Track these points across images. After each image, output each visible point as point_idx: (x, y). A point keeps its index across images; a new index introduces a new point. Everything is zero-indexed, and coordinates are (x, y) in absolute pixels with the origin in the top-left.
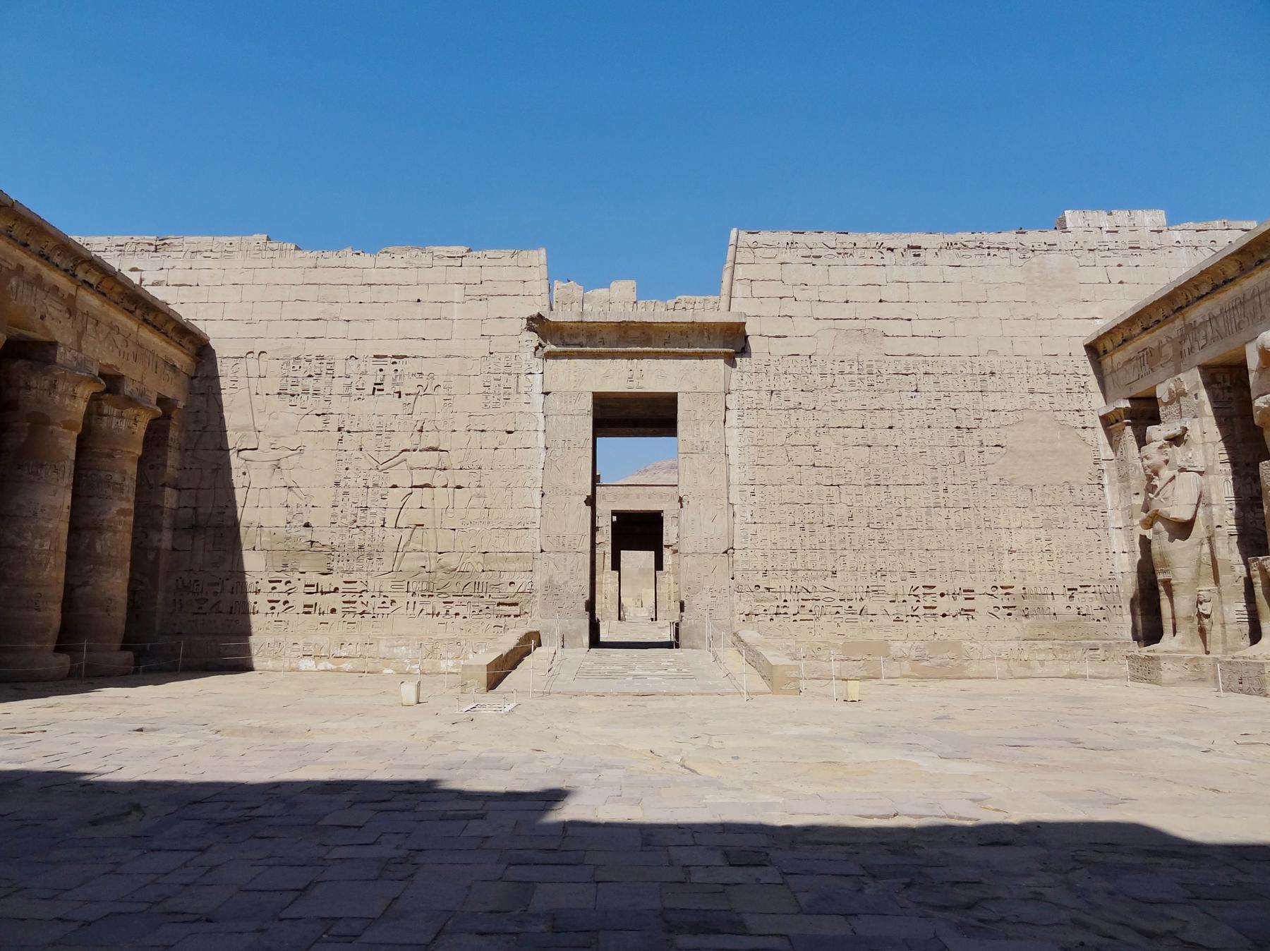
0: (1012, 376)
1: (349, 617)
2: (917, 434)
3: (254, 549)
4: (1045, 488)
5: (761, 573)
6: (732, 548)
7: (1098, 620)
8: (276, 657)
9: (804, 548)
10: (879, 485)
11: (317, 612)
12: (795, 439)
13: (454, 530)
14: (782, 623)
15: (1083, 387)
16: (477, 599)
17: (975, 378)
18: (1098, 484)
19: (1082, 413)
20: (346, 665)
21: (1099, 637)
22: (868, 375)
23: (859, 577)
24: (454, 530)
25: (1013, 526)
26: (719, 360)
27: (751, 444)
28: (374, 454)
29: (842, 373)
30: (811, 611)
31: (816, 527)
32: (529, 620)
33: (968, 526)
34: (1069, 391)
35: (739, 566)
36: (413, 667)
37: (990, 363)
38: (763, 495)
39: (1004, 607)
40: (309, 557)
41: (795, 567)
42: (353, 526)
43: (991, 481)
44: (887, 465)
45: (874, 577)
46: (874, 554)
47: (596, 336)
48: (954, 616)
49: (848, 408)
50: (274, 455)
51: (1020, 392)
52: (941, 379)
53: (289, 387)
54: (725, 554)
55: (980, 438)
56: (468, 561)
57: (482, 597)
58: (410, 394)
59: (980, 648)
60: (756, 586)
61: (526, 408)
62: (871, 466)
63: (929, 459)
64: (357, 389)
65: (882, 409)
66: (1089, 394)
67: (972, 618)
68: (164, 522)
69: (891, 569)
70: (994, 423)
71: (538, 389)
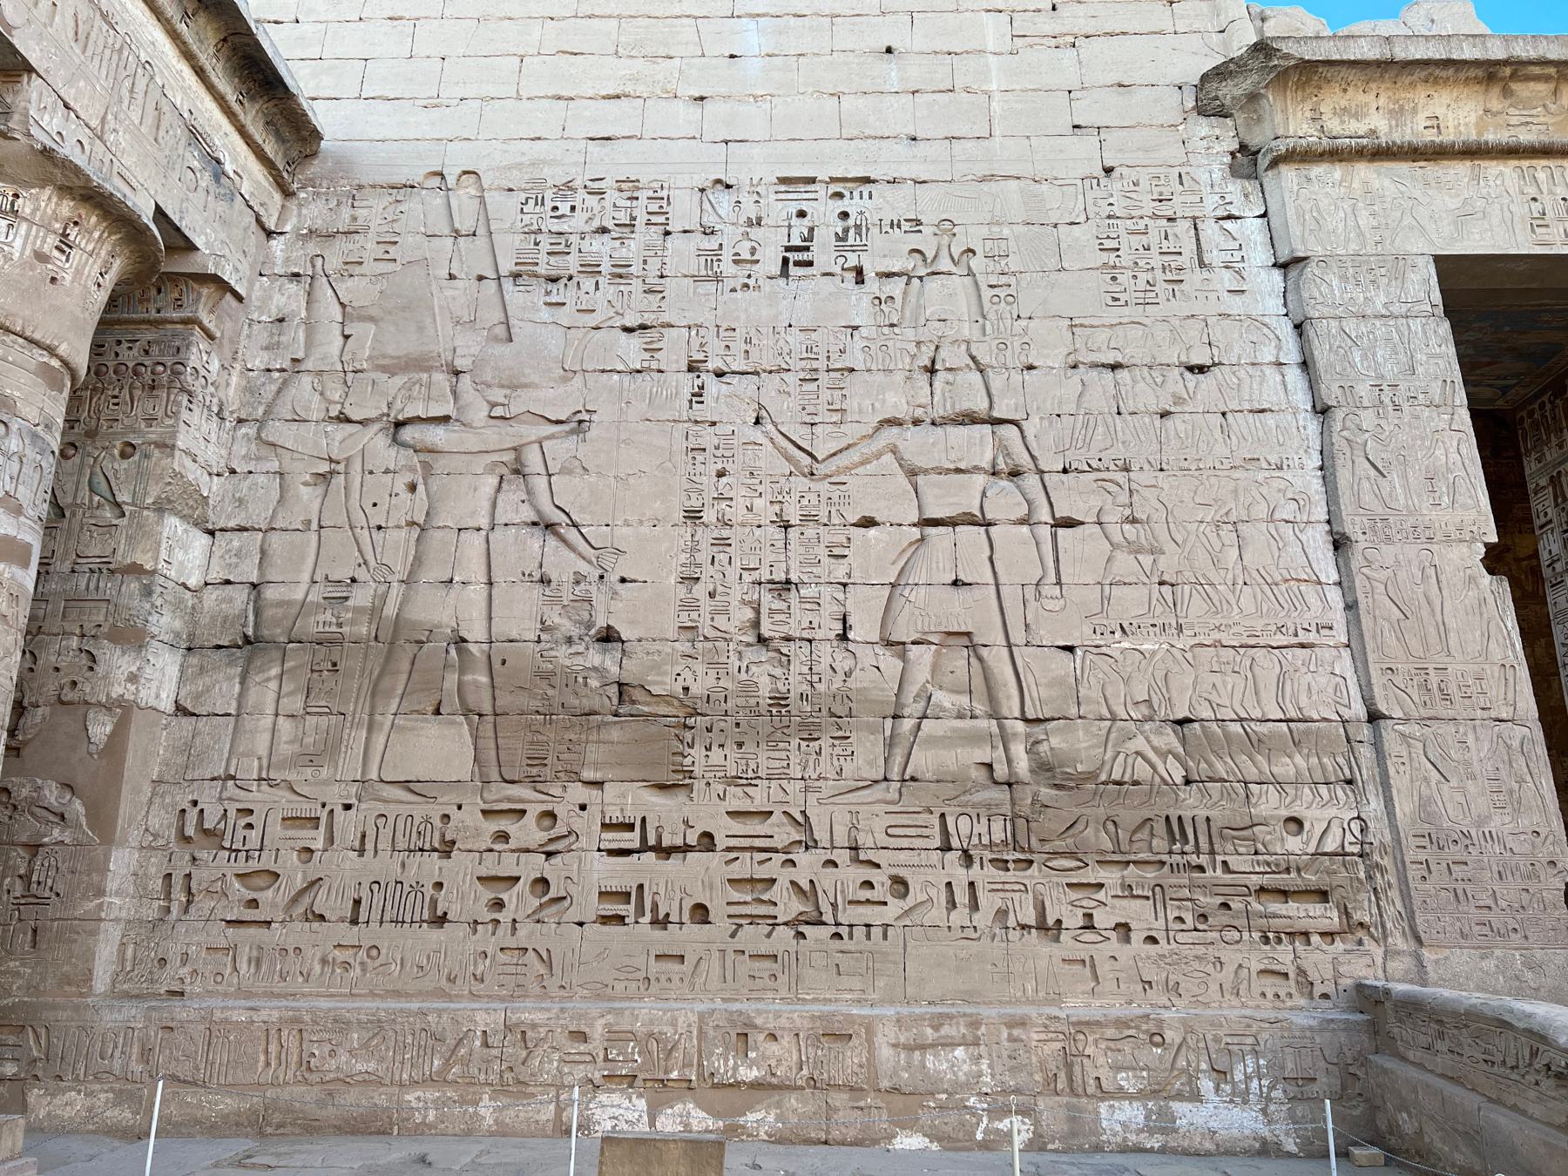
1: (751, 936)
3: (437, 712)
8: (515, 1087)
11: (648, 918)
13: (1070, 649)
16: (1183, 878)
20: (759, 1116)
24: (1070, 649)
28: (800, 434)
32: (1378, 952)
36: (1001, 1126)
40: (615, 734)
42: (744, 638)
47: (1415, 111)
50: (497, 436)
53: (543, 258)
56: (1132, 746)
57: (1201, 869)
58: (889, 275)
61: (1235, 305)
64: (735, 262)
68: (154, 618)
71: (1260, 255)
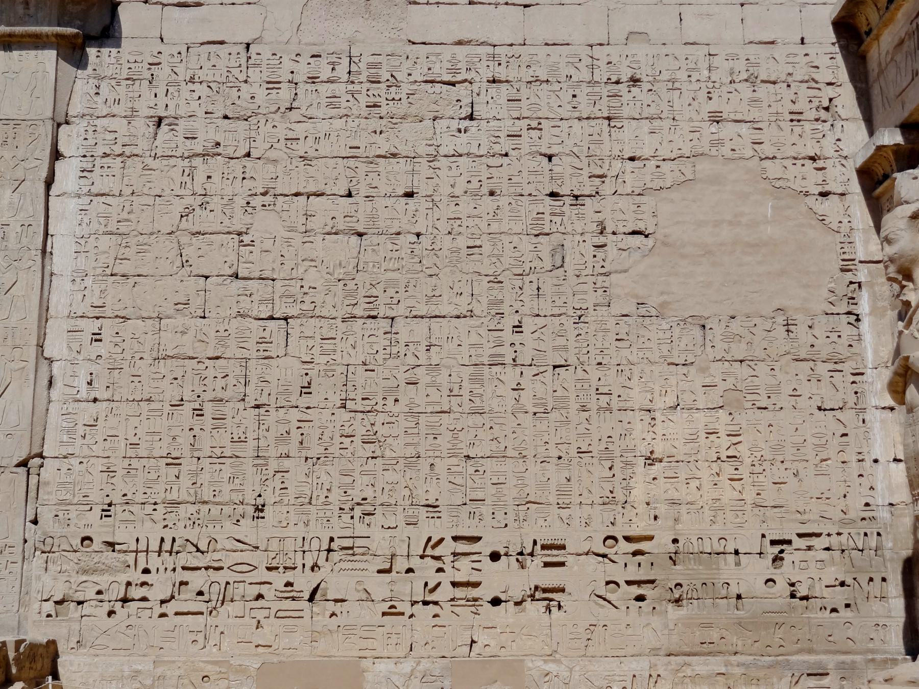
0: (677, 85)
2: (466, 207)
4: (735, 326)
5: (97, 510)
6: (41, 456)
7: (834, 610)
9: (196, 454)
10: (374, 317)
12: (203, 220)
14: (133, 621)
15: (827, 109)
17: (597, 89)
18: (849, 313)
19: (820, 164)
21: (833, 647)
22: (368, 85)
23: (313, 517)
25: (659, 404)
26: (46, 52)
27: (102, 229)
29: (313, 80)
30: (200, 593)
31: (228, 409)
33: (561, 404)
34: (795, 117)
35: (49, 495)
37: (630, 59)
38: (118, 339)
39: (629, 583)
41: (174, 496)
43: (616, 309)
44: (395, 275)
45: (346, 518)
46: (350, 466)
48: (517, 604)
49: (322, 152)
51: (691, 120)
52: (525, 92)
54: (22, 470)
55: (600, 217)
59: (567, 674)
60: (84, 539)
62: (359, 277)
63: (486, 261)
65: (394, 155)
66: (838, 124)
67: (560, 607)
69: (384, 498)
70: (631, 182)
